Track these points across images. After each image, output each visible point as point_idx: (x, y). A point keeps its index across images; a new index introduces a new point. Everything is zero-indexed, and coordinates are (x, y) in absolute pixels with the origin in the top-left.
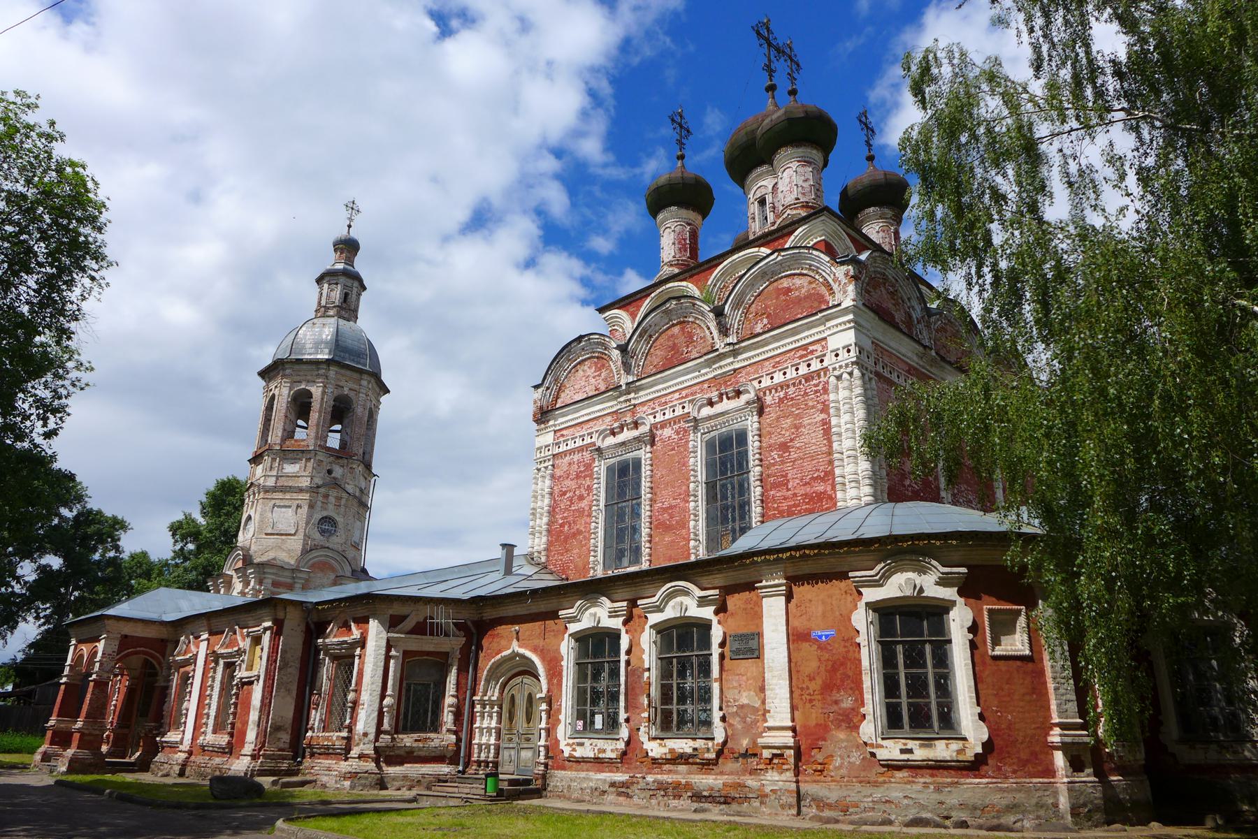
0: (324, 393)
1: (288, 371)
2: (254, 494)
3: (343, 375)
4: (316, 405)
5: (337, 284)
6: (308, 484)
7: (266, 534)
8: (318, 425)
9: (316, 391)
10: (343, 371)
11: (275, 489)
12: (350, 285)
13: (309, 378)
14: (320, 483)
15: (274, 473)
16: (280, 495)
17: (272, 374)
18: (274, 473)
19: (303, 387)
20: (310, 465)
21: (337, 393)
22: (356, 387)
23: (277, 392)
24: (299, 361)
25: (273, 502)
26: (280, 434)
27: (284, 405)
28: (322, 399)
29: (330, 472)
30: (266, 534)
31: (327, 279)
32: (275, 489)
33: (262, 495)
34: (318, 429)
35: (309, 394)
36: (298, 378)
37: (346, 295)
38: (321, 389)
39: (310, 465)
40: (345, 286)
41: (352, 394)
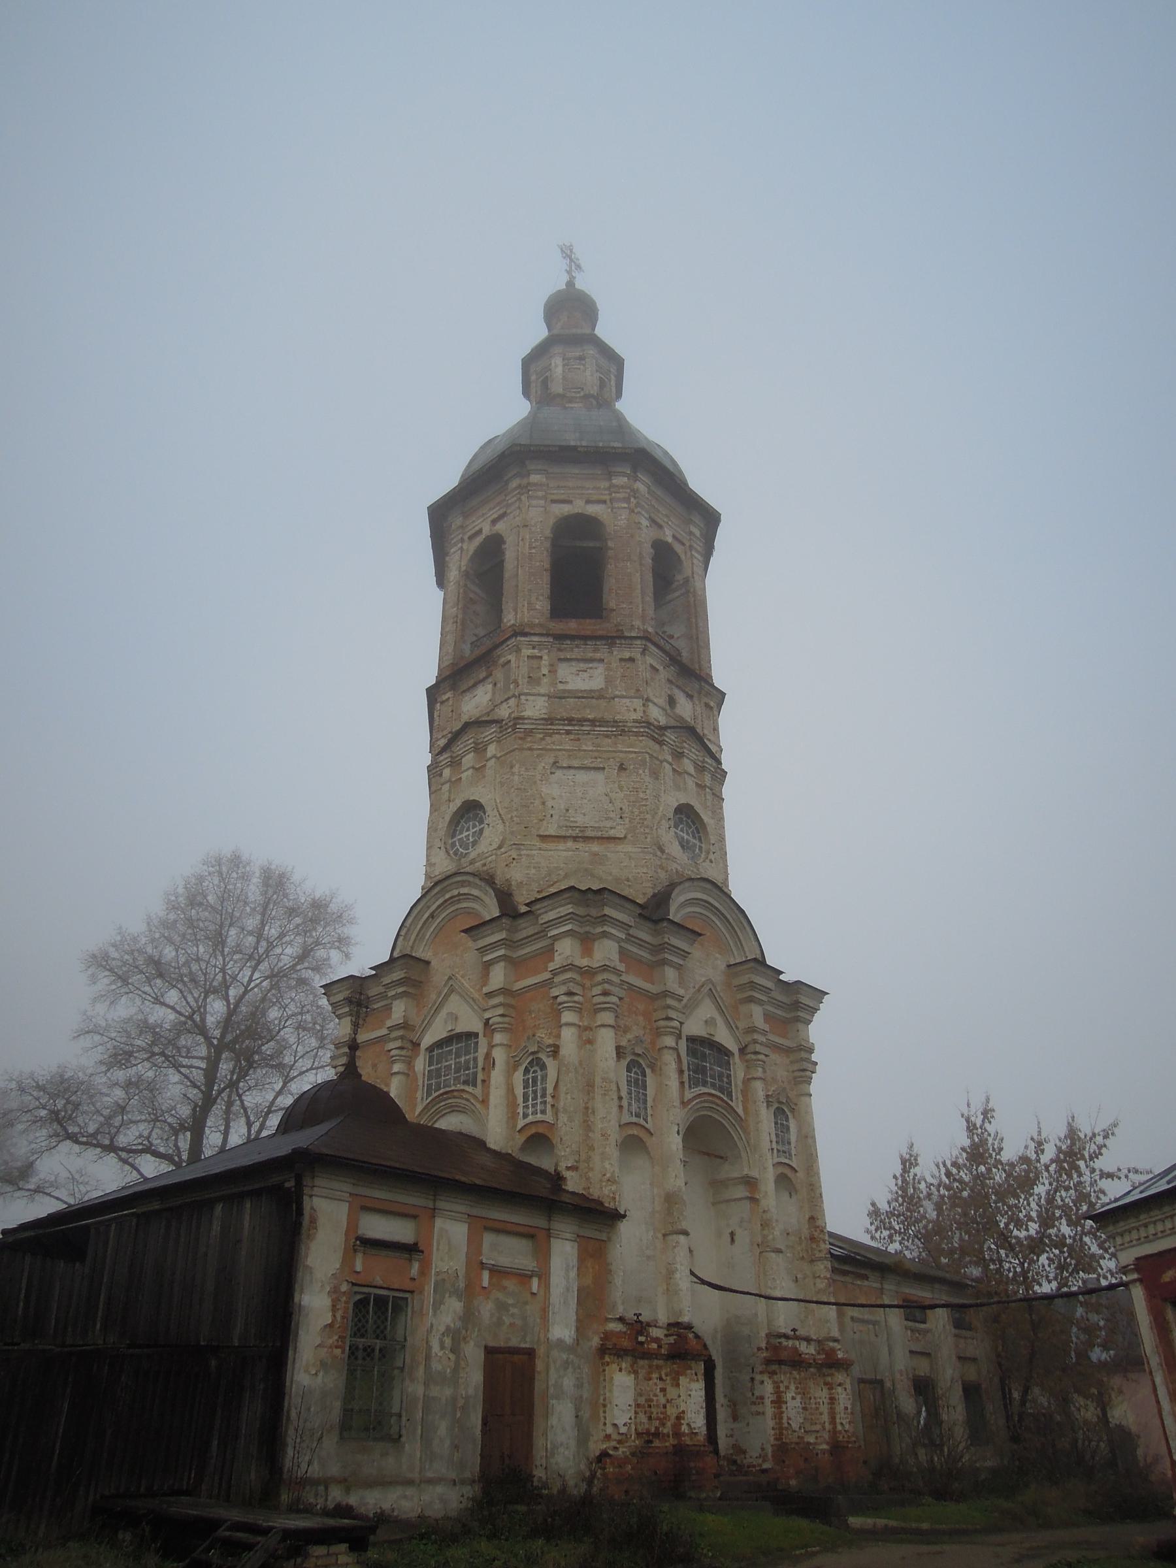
2: (479, 749)
7: (544, 838)
31: (558, 349)
41: (678, 548)
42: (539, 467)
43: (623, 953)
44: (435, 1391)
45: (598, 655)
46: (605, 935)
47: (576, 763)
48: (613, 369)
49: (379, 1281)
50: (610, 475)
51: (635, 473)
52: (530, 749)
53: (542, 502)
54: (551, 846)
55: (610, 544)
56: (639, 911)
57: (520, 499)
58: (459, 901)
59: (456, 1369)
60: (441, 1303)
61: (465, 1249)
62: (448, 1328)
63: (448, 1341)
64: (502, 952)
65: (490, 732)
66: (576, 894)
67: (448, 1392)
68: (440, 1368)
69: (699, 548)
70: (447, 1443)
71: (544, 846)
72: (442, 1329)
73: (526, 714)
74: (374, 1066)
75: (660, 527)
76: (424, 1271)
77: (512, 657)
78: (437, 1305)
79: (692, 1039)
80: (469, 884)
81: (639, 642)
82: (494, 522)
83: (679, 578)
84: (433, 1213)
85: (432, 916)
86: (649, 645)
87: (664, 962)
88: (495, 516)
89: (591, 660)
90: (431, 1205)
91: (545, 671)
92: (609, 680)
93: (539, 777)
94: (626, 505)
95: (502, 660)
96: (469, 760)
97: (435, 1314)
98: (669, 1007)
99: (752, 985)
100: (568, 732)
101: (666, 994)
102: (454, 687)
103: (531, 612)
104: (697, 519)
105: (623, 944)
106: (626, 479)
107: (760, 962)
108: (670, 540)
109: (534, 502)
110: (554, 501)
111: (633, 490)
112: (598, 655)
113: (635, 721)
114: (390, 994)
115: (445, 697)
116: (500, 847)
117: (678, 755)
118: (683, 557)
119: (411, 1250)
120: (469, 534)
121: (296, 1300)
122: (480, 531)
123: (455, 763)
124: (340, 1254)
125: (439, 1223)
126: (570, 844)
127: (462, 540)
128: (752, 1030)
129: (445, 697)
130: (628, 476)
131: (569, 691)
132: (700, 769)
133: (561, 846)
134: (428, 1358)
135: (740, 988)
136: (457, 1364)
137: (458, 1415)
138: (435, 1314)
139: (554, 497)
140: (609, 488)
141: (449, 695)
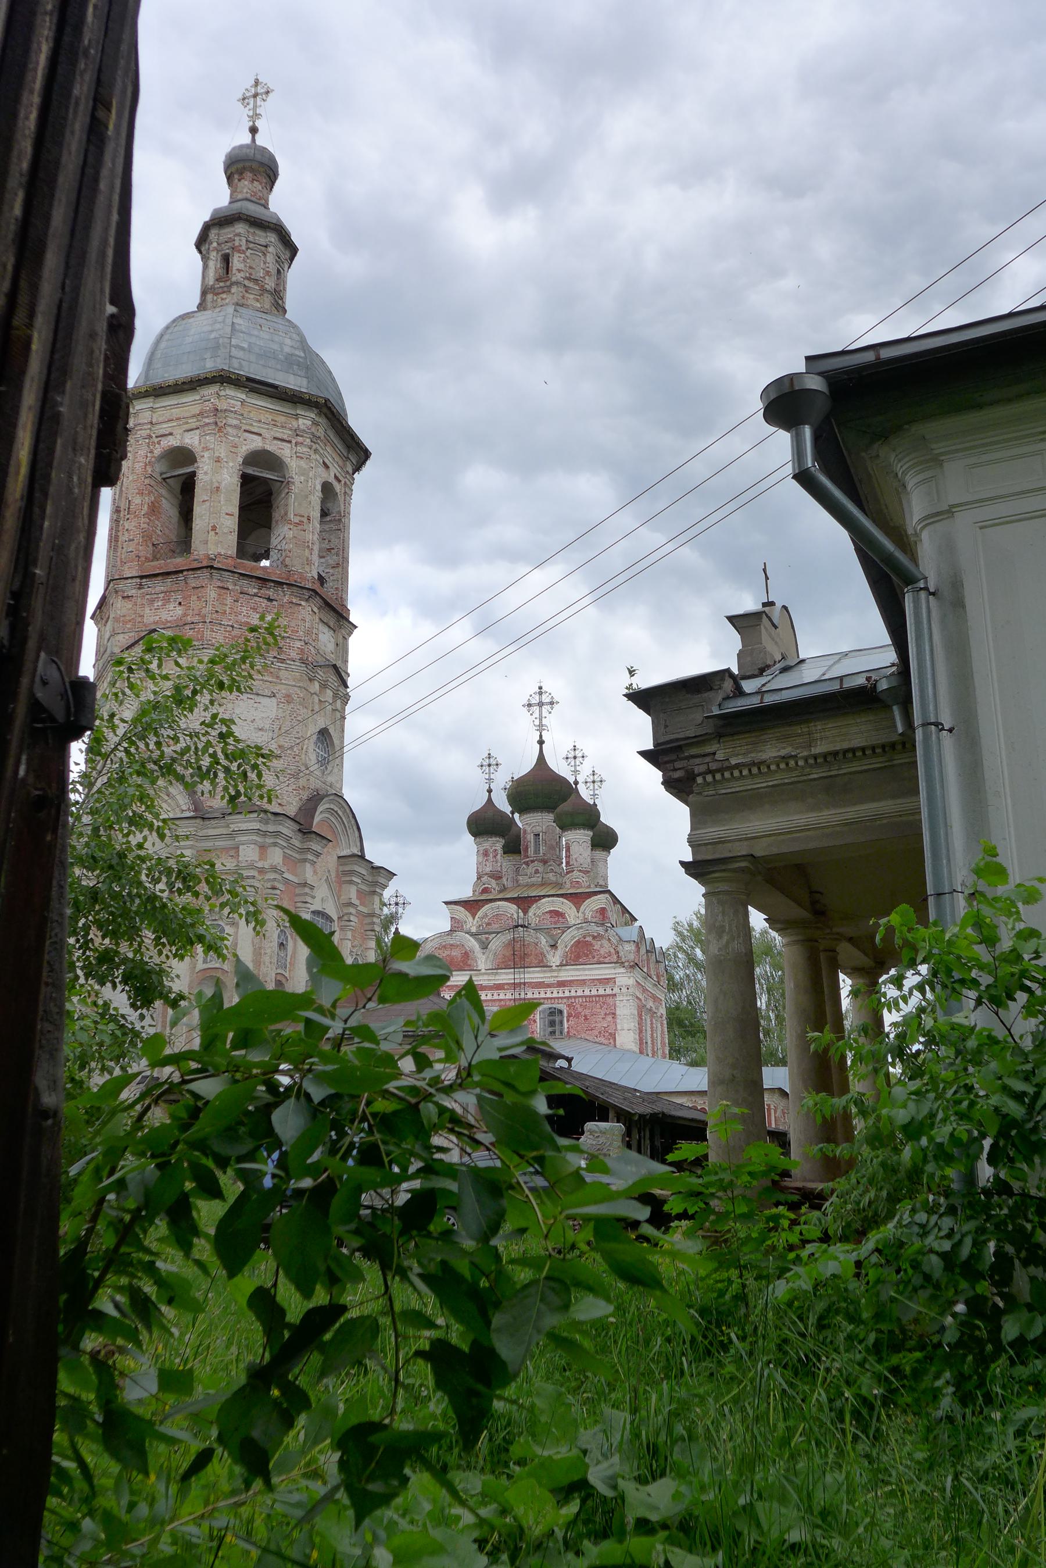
43: (286, 857)
46: (275, 844)
48: (288, 255)
56: (297, 827)
75: (327, 467)
79: (313, 912)
87: (305, 860)
98: (306, 894)
99: (352, 872)
101: (305, 884)
105: (286, 851)
107: (362, 857)
117: (324, 686)
127: (150, 437)
128: (350, 904)
132: (336, 696)
135: (346, 873)
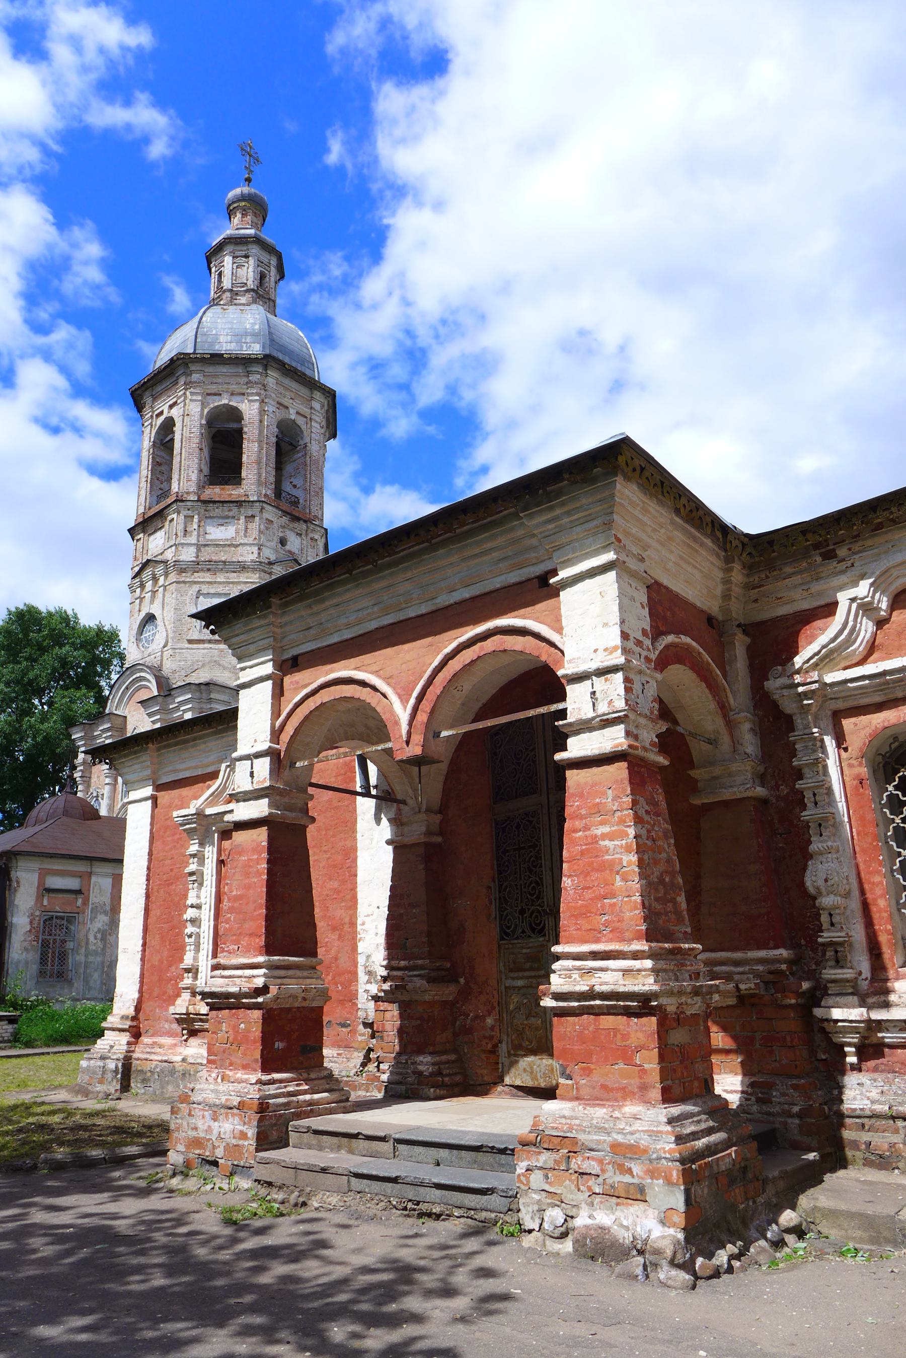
0: (262, 412)
1: (195, 377)
2: (155, 579)
3: (286, 389)
4: (251, 431)
5: (247, 257)
6: (254, 557)
7: (190, 642)
8: (259, 462)
9: (249, 409)
10: (287, 381)
11: (197, 566)
12: (266, 261)
13: (234, 387)
14: (273, 558)
15: (193, 539)
16: (207, 577)
17: (159, 388)
18: (193, 539)
19: (225, 401)
20: (255, 526)
21: (281, 415)
22: (306, 411)
23: (175, 413)
24: (216, 359)
25: (196, 588)
26: (194, 477)
27: (196, 431)
28: (261, 421)
29: (283, 542)
30: (190, 642)
31: (229, 248)
32: (197, 566)
33: (173, 577)
34: (259, 469)
35: (235, 415)
36: (213, 388)
37: (262, 277)
38: (257, 405)
39: (255, 526)
40: (260, 262)
41: (300, 421)
42: (198, 368)
44: (91, 959)
45: (231, 514)
47: (212, 591)
49: (58, 909)
50: (248, 373)
51: (266, 370)
52: (184, 582)
53: (200, 398)
54: (195, 646)
55: (245, 429)
57: (185, 394)
58: (141, 681)
59: (103, 949)
60: (96, 917)
61: (110, 891)
62: (99, 930)
63: (99, 936)
64: (158, 717)
65: (159, 570)
66: (193, 687)
67: (99, 959)
68: (94, 948)
69: (318, 419)
70: (98, 982)
71: (190, 646)
72: (96, 930)
73: (182, 558)
74: (98, 777)
76: (86, 902)
77: (175, 516)
78: (92, 920)
80: (145, 671)
81: (258, 504)
82: (171, 407)
83: (301, 442)
84: (90, 874)
85: (127, 688)
86: (265, 505)
88: (171, 402)
89: (227, 517)
90: (89, 870)
91: (195, 526)
92: (237, 532)
93: (188, 601)
94: (257, 398)
95: (169, 518)
96: (149, 585)
97: (91, 923)
100: (209, 570)
102: (144, 532)
103: (189, 483)
104: (317, 395)
106: (258, 376)
108: (293, 417)
109: (194, 398)
110: (208, 394)
111: (264, 385)
112: (231, 514)
113: (252, 561)
114: (104, 735)
115: (138, 537)
116: (164, 647)
118: (303, 427)
119: (78, 892)
120: (156, 413)
121: (9, 920)
122: (162, 413)
123: (142, 586)
124: (34, 898)
125: (93, 879)
126: (206, 645)
127: (152, 416)
129: (138, 537)
130: (261, 374)
131: (211, 540)
133: (201, 646)
134: (87, 943)
136: (105, 946)
137: (106, 969)
138: (91, 923)
139: (209, 391)
140: (247, 383)
141: (141, 535)
